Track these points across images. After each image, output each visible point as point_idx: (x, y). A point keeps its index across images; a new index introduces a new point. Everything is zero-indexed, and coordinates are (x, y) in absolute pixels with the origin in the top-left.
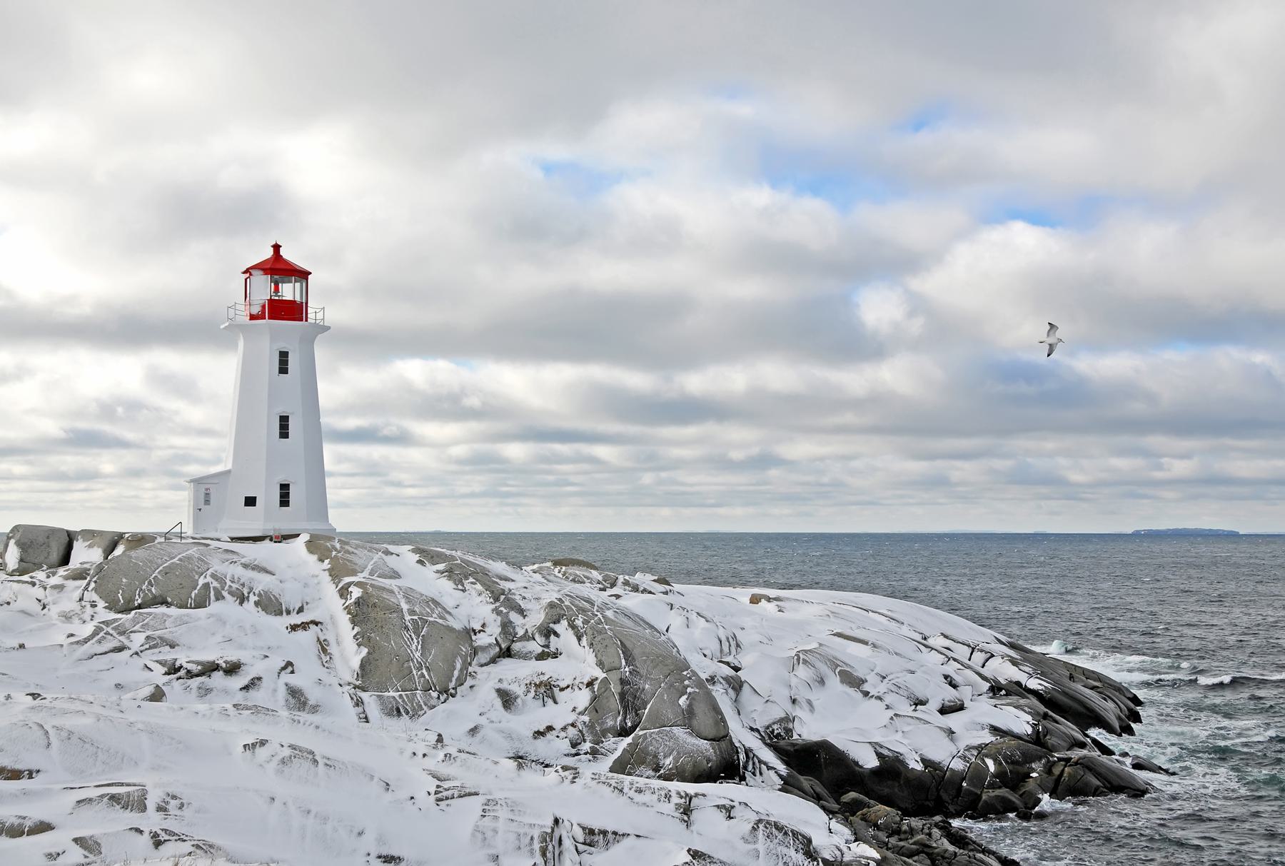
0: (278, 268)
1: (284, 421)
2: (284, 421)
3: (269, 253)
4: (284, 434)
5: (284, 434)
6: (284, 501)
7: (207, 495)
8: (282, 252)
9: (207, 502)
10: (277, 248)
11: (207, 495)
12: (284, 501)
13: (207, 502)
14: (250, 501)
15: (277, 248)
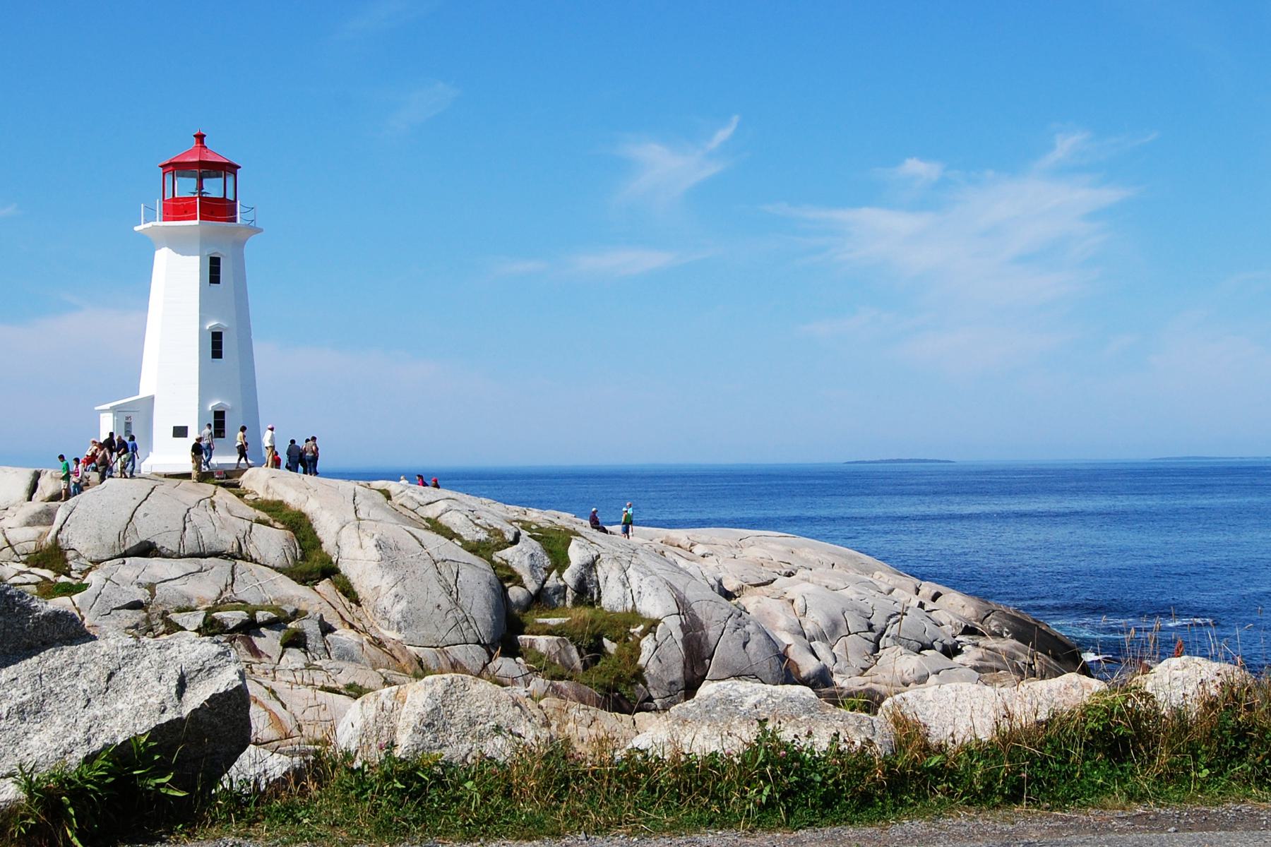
1: (217, 338)
2: (217, 338)
10: (200, 138)
14: (180, 432)
15: (200, 138)
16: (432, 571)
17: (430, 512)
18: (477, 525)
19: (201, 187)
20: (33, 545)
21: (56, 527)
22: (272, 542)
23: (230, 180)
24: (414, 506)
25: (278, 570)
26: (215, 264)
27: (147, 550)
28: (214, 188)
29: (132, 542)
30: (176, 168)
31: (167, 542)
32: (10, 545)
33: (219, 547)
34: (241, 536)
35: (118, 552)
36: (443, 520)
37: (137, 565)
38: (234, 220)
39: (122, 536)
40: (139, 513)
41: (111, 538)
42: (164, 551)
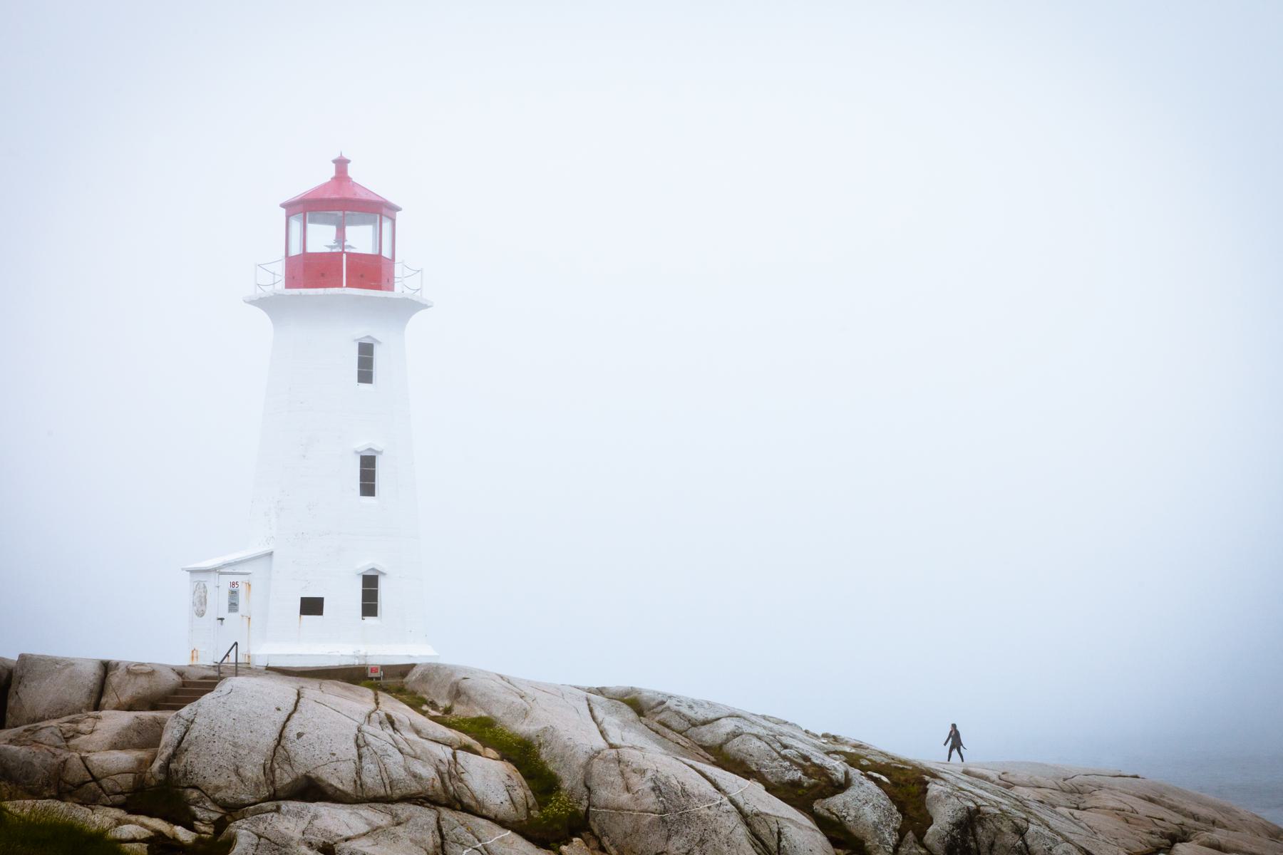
0: (338, 201)
1: (368, 466)
2: (368, 466)
3: (329, 173)
4: (368, 487)
5: (368, 487)
6: (370, 607)
7: (233, 594)
8: (352, 172)
9: (233, 606)
10: (341, 164)
11: (233, 594)
12: (370, 607)
13: (233, 606)
14: (312, 606)
15: (341, 164)
16: (742, 830)
17: (710, 735)
18: (785, 758)
19: (341, 236)
20: (130, 778)
21: (165, 752)
22: (488, 777)
23: (387, 225)
24: (683, 725)
25: (502, 823)
26: (366, 353)
27: (311, 790)
28: (360, 239)
29: (285, 777)
30: (308, 207)
31: (339, 776)
32: (95, 779)
33: (415, 787)
34: (443, 768)
35: (264, 792)
36: (733, 747)
37: (298, 815)
38: (392, 289)
39: (269, 770)
40: (291, 732)
41: (253, 771)
42: (330, 791)
